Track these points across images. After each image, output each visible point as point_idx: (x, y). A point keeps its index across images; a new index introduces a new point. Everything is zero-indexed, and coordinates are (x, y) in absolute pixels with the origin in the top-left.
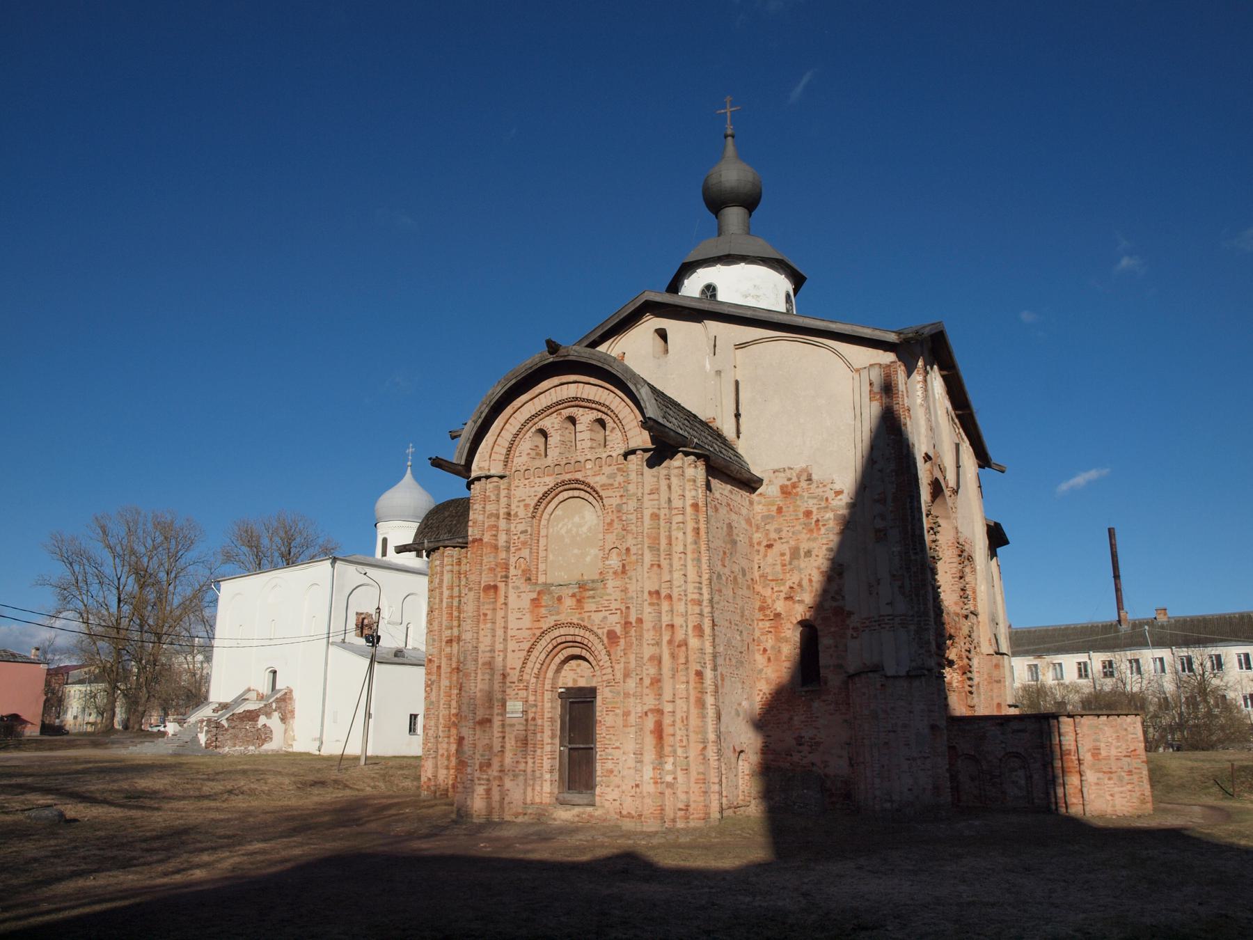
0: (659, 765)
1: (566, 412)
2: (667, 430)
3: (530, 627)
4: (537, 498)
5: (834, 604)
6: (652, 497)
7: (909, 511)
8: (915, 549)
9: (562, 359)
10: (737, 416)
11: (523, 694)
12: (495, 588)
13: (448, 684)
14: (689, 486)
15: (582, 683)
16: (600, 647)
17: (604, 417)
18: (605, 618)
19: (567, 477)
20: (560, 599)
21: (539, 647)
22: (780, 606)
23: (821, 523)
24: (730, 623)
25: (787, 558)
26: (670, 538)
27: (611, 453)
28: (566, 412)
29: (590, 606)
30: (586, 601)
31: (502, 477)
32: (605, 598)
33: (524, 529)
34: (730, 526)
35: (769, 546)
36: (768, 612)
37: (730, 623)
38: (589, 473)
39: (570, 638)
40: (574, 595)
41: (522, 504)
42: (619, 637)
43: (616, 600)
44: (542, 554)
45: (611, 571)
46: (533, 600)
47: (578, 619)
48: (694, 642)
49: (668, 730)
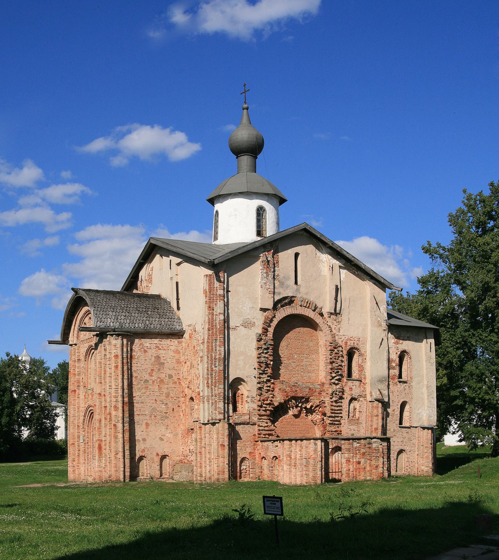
0: (100, 461)
2: (93, 329)
5: (198, 390)
6: (100, 354)
7: (214, 347)
8: (215, 365)
10: (178, 299)
11: (84, 433)
12: (75, 391)
14: (113, 348)
22: (186, 390)
23: (197, 352)
24: (156, 400)
25: (189, 368)
26: (105, 371)
31: (76, 345)
34: (158, 357)
35: (185, 363)
36: (183, 393)
37: (156, 400)
44: (89, 376)
46: (85, 395)
48: (114, 413)
49: (103, 447)
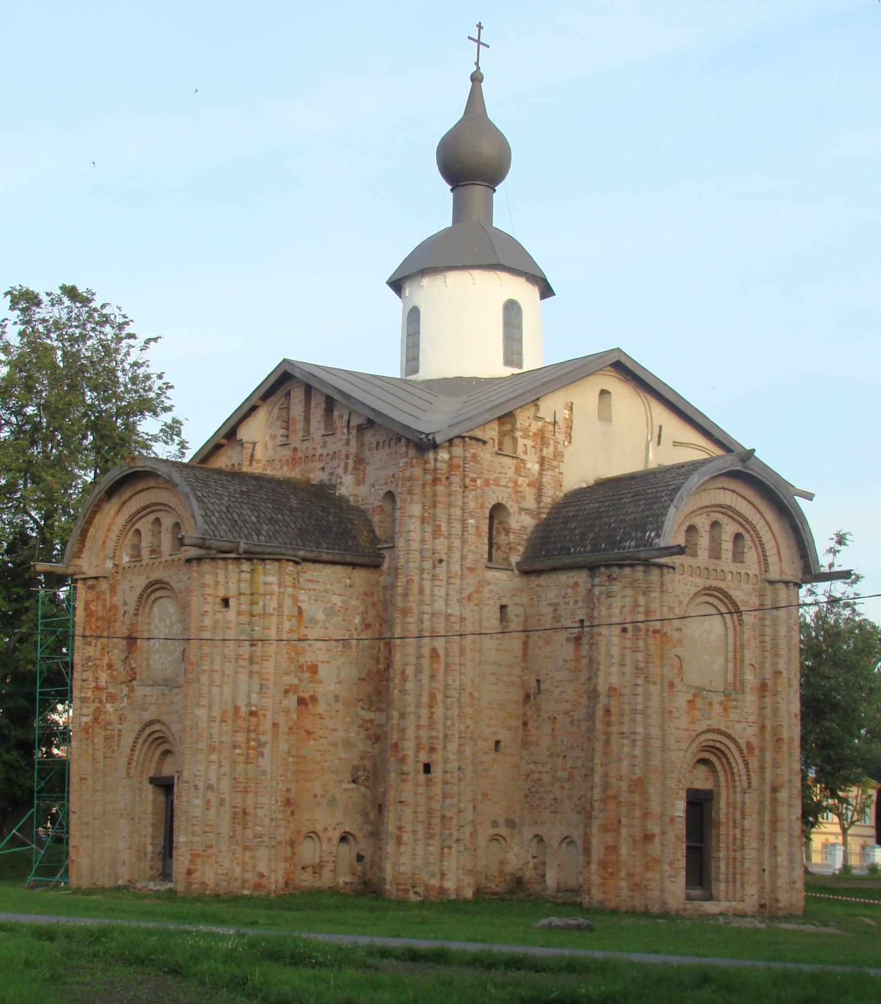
1: (715, 516)
3: (685, 728)
4: (689, 597)
9: (746, 471)
13: (287, 749)
15: (698, 785)
16: (737, 755)
17: (744, 533)
18: (744, 729)
19: (714, 583)
20: (710, 704)
21: (691, 750)
27: (748, 571)
28: (715, 516)
29: (734, 715)
30: (732, 710)
32: (745, 710)
33: (679, 627)
38: (731, 585)
39: (711, 743)
40: (721, 703)
41: (677, 599)
42: (754, 749)
43: (752, 714)
45: (749, 686)
46: (690, 702)
47: (726, 727)
